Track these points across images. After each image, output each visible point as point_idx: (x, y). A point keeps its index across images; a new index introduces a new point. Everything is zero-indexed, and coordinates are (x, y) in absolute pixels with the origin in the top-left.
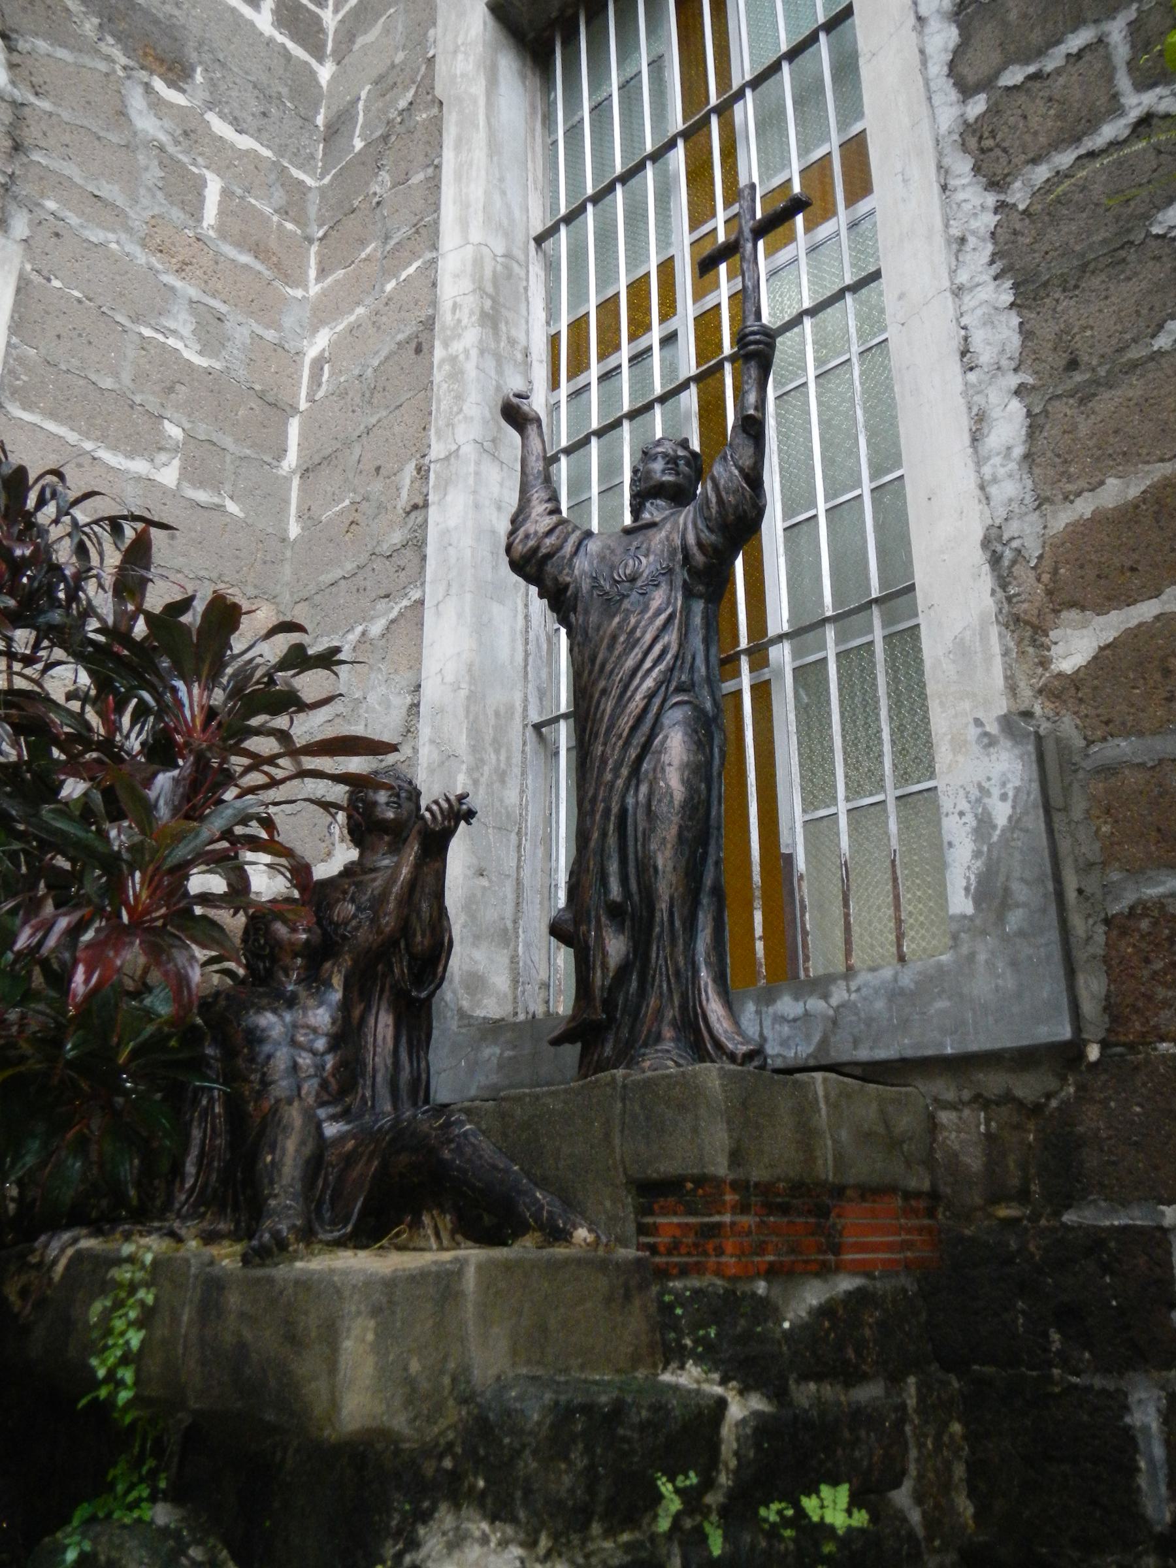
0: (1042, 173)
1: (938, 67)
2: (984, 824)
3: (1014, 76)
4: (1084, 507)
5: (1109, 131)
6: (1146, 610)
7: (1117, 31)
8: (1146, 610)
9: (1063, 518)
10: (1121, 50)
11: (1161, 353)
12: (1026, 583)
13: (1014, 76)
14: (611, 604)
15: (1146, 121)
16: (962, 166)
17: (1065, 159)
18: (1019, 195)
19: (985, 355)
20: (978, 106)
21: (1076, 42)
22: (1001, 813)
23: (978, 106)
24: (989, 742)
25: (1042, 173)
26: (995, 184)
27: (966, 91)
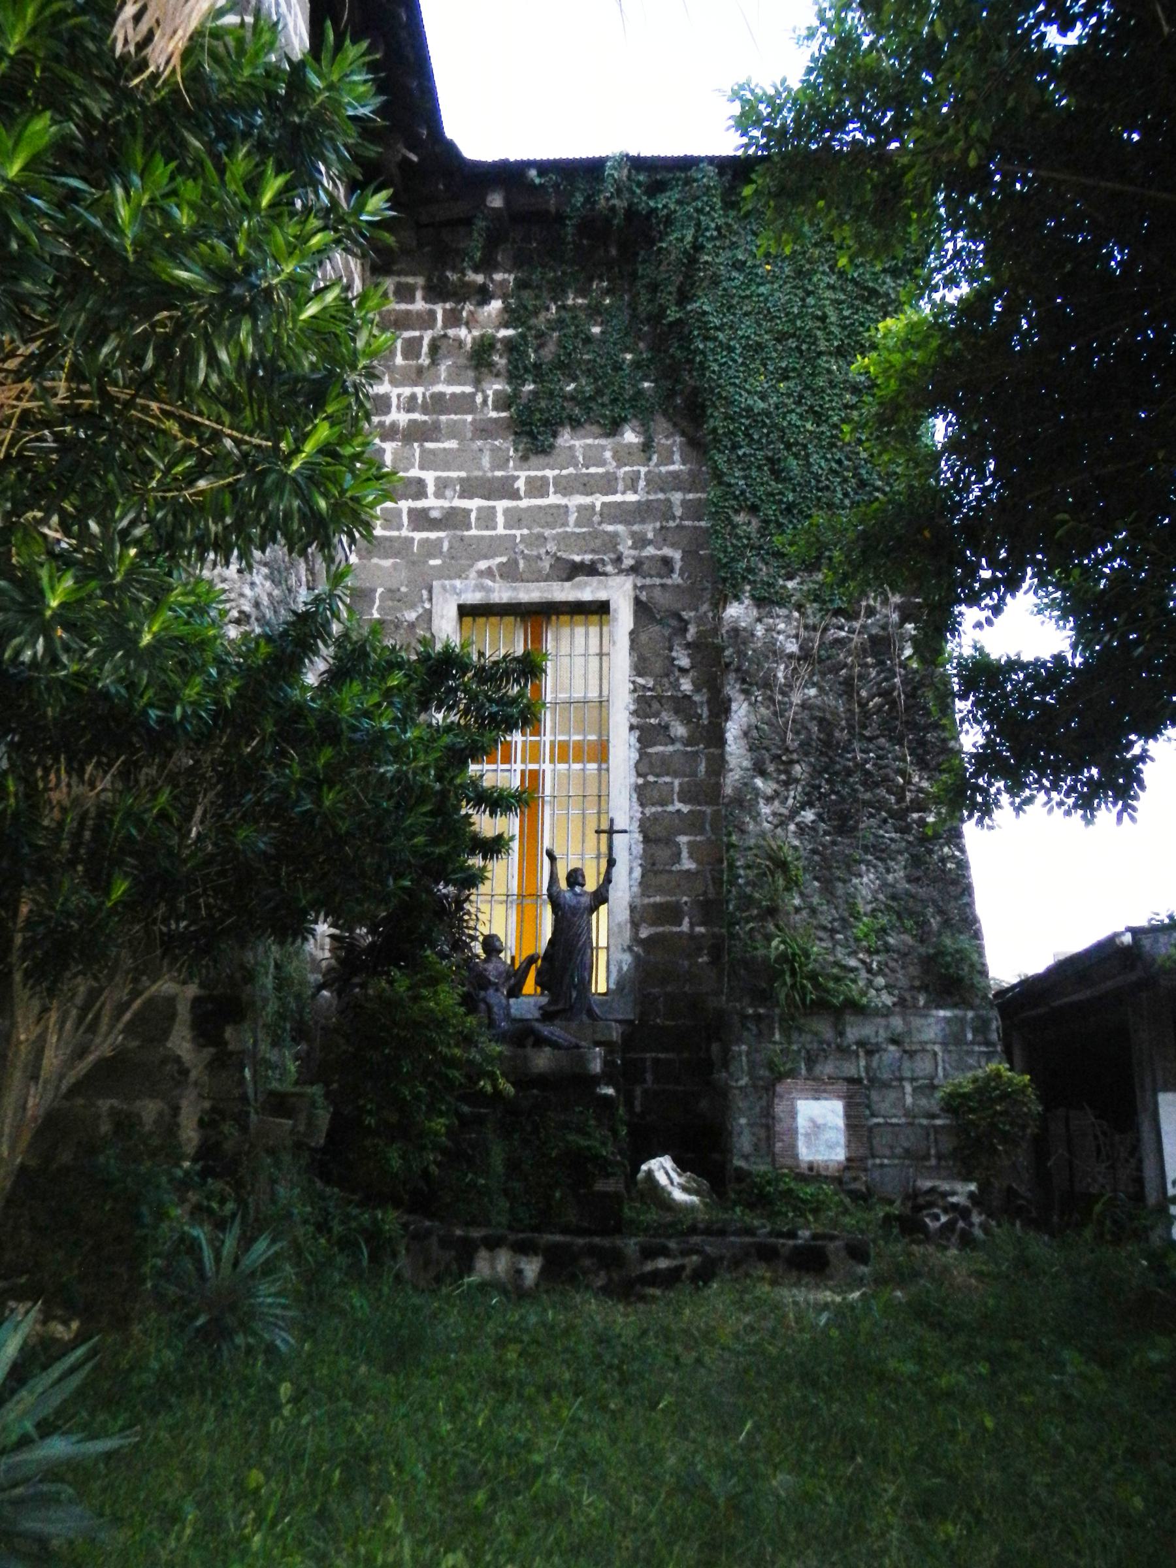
0: (653, 809)
1: (632, 762)
2: (620, 969)
3: (651, 778)
4: (652, 900)
5: (670, 808)
6: (660, 929)
7: (677, 782)
8: (660, 929)
9: (646, 901)
10: (677, 789)
11: (671, 872)
12: (637, 916)
13: (651, 778)
14: (574, 915)
15: (678, 811)
16: (635, 796)
17: (660, 809)
18: (649, 811)
19: (635, 852)
20: (640, 781)
21: (668, 779)
22: (625, 968)
23: (640, 781)
24: (624, 950)
25: (653, 809)
26: (642, 805)
27: (639, 775)
